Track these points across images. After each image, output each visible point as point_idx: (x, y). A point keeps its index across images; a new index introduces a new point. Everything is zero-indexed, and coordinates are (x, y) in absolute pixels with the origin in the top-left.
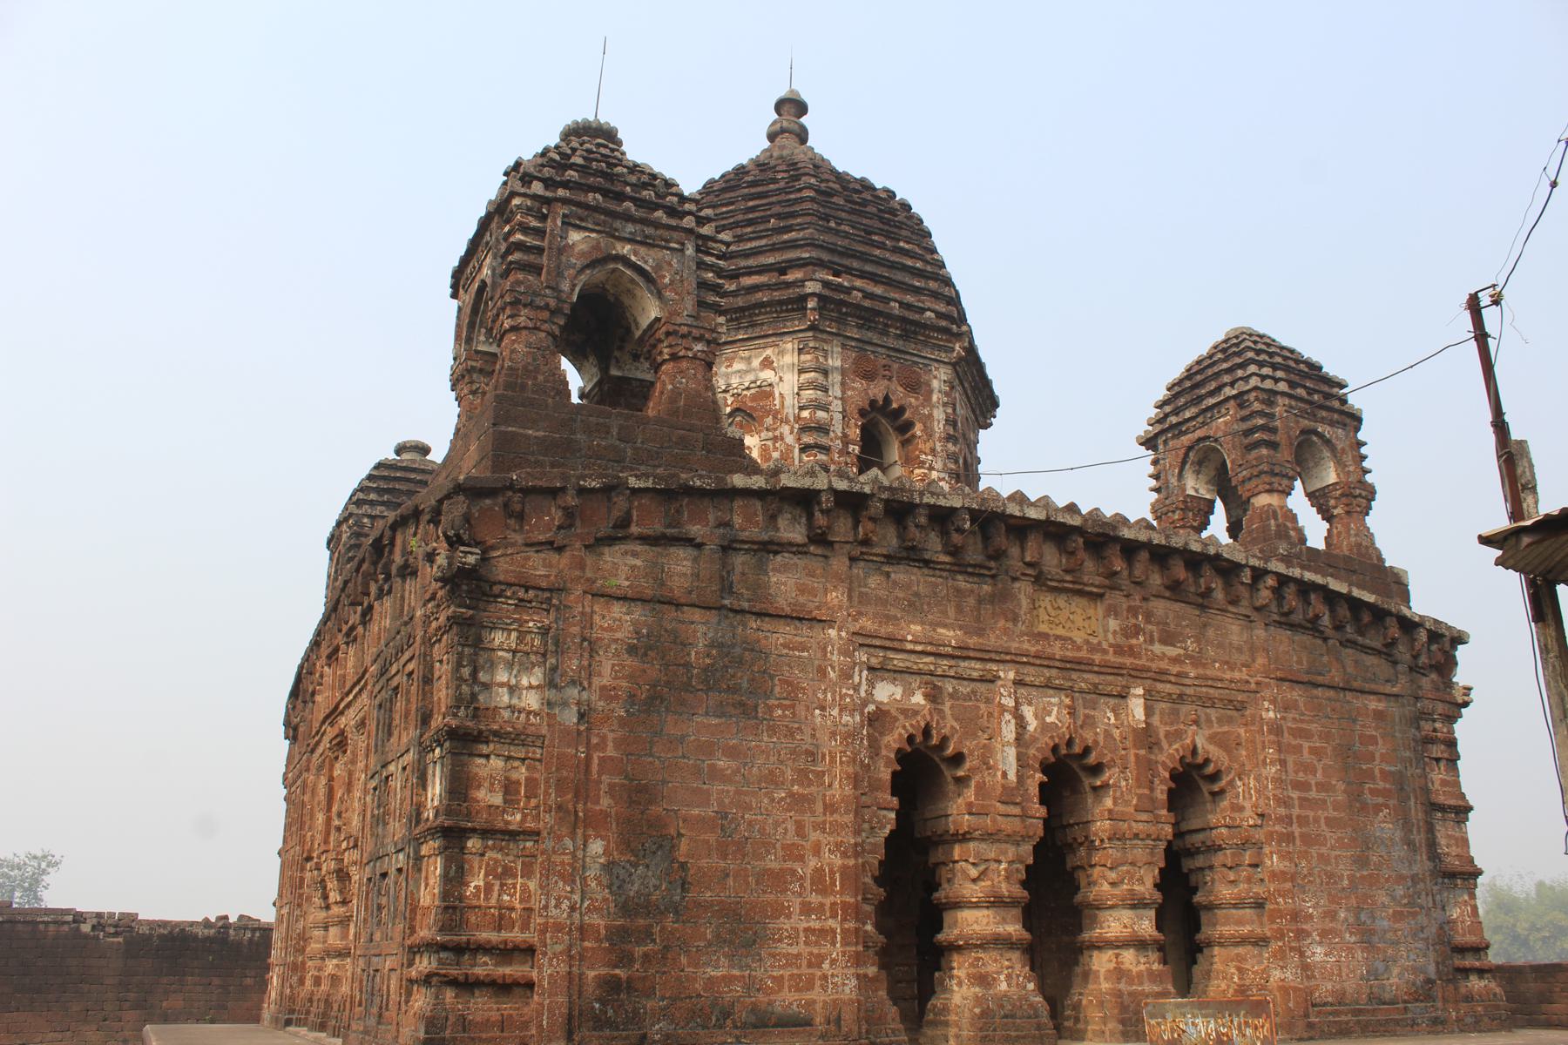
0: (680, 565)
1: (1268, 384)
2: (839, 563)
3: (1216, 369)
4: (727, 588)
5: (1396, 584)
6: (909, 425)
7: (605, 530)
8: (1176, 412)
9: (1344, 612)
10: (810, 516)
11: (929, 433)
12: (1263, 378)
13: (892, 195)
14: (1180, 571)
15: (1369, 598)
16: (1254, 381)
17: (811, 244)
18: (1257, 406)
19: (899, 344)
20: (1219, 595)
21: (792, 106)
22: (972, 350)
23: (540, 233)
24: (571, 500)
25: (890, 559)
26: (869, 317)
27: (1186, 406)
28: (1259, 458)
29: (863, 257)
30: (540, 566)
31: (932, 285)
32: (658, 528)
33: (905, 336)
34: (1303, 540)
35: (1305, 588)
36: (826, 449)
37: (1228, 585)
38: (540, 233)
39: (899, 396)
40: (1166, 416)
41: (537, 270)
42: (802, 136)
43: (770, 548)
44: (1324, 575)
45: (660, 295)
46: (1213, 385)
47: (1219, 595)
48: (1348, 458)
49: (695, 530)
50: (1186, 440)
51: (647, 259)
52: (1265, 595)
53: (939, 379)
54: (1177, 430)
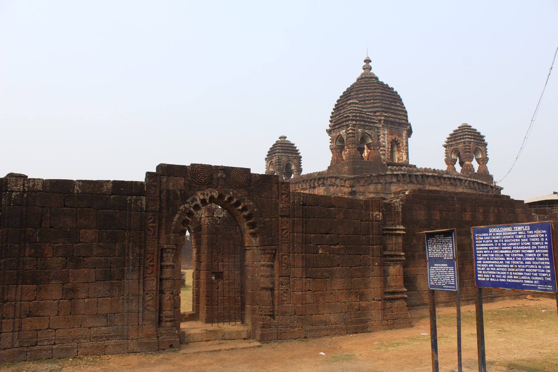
0: (379, 186)
1: (470, 140)
2: (401, 184)
3: (459, 134)
4: (386, 190)
5: (490, 178)
6: (399, 144)
7: (370, 182)
8: (451, 141)
9: (480, 186)
10: (397, 178)
11: (403, 145)
12: (469, 138)
13: (393, 89)
14: (453, 181)
15: (485, 183)
16: (467, 139)
17: (381, 107)
18: (467, 144)
19: (397, 127)
20: (459, 184)
21: (368, 61)
22: (411, 127)
23: (354, 130)
24: (366, 179)
25: (408, 183)
26: (392, 123)
27: (453, 141)
28: (467, 155)
29: (391, 109)
30: (362, 189)
31: (403, 113)
32: (376, 181)
33: (398, 126)
34: (474, 170)
35: (474, 182)
36: (385, 150)
37: (460, 182)
38: (354, 130)
39: (398, 138)
40: (449, 142)
41: (354, 137)
42: (370, 69)
43: (391, 183)
44: (477, 179)
45: (371, 138)
46: (459, 138)
47: (459, 184)
48: (484, 153)
49: (381, 181)
50: (453, 148)
51: (369, 132)
52: (467, 184)
53: (404, 134)
54: (451, 145)
